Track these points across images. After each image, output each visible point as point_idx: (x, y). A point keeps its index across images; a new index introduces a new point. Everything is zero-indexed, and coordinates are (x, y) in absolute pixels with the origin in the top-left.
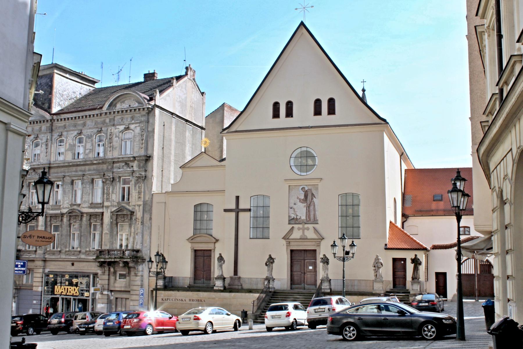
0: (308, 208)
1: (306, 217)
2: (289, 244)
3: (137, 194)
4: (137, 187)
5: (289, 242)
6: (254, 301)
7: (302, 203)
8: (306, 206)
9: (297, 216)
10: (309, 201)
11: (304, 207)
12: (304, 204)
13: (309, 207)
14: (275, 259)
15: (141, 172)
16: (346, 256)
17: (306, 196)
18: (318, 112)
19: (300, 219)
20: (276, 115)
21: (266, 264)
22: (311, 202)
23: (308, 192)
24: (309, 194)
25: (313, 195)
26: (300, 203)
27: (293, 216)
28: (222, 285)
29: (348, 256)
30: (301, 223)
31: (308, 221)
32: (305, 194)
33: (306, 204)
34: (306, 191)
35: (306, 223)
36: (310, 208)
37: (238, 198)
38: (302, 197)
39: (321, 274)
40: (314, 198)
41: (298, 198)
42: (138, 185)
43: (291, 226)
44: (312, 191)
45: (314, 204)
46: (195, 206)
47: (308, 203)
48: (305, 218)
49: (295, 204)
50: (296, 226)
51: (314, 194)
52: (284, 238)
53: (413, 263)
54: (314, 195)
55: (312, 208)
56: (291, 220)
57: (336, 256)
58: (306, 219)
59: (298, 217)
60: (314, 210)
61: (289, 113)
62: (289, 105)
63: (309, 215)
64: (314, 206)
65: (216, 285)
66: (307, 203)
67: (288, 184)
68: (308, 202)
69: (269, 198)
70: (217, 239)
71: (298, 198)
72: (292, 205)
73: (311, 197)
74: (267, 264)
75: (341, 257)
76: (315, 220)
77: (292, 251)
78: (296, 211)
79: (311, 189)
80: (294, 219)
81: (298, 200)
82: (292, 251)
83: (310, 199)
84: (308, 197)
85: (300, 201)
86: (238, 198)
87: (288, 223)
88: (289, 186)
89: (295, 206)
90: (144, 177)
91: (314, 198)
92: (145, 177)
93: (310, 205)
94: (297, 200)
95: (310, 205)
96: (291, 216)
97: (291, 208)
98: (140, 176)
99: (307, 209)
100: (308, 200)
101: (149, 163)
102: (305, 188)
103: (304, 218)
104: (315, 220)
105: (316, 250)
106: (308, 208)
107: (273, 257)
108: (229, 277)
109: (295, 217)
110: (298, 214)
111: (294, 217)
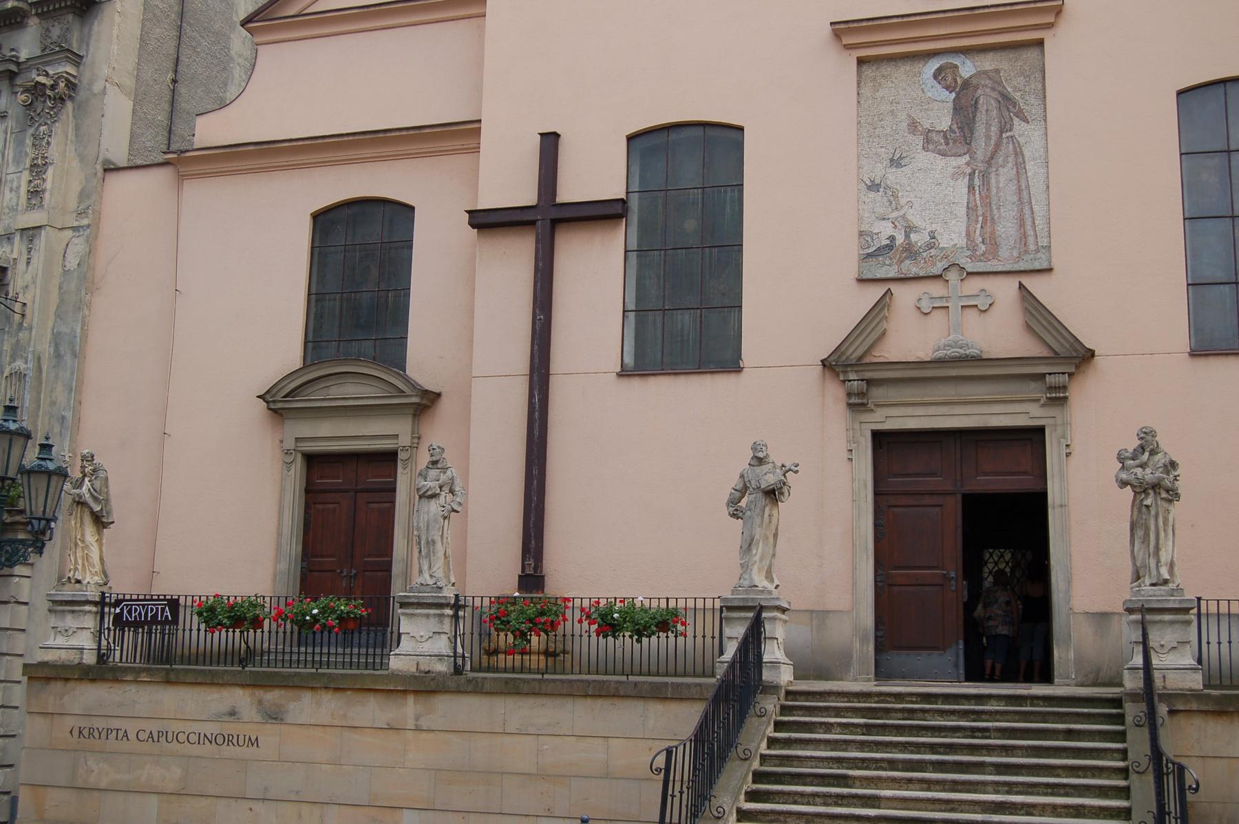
0: (977, 182)
1: (968, 235)
2: (858, 404)
3: (26, 176)
4: (29, 141)
5: (869, 382)
6: (669, 752)
7: (944, 155)
8: (968, 170)
9: (909, 229)
10: (988, 137)
11: (955, 176)
13: (985, 176)
15: (48, 63)
17: (965, 111)
19: (930, 246)
21: (733, 502)
22: (998, 145)
23: (976, 88)
25: (1006, 100)
26: (931, 155)
27: (885, 230)
30: (937, 270)
31: (984, 257)
33: (967, 157)
34: (966, 84)
36: (993, 176)
37: (550, 142)
38: (944, 121)
40: (1016, 121)
41: (913, 126)
42: (31, 131)
43: (876, 292)
44: (1000, 83)
45: (1018, 153)
46: (316, 217)
47: (980, 154)
48: (962, 242)
49: (896, 162)
50: (905, 296)
51: (1017, 96)
52: (833, 366)
54: (1015, 104)
55: (1003, 177)
56: (869, 255)
58: (971, 246)
59: (918, 239)
63: (989, 220)
64: (1020, 167)
67: (848, 47)
68: (981, 148)
69: (740, 146)
71: (913, 126)
72: (878, 171)
73: (995, 113)
74: (743, 503)
76: (1026, 252)
77: (881, 439)
78: (903, 201)
79: (997, 71)
80: (890, 247)
81: (919, 141)
82: (881, 439)
83: (994, 129)
84: (981, 117)
85: (928, 141)
86: (550, 142)
87: (854, 274)
88: (861, 62)
89: (894, 177)
90: (62, 85)
91: (1016, 121)
92: (71, 86)
93: (989, 161)
94: (910, 137)
95: (989, 161)
96: (871, 234)
97: (874, 187)
98: (42, 79)
99: (971, 188)
100: (980, 130)
101: (96, 23)
102: (956, 67)
103: (953, 236)
104: (1026, 252)
105: (1041, 430)
106: (977, 182)
109: (900, 239)
110: (916, 220)
111: (892, 238)
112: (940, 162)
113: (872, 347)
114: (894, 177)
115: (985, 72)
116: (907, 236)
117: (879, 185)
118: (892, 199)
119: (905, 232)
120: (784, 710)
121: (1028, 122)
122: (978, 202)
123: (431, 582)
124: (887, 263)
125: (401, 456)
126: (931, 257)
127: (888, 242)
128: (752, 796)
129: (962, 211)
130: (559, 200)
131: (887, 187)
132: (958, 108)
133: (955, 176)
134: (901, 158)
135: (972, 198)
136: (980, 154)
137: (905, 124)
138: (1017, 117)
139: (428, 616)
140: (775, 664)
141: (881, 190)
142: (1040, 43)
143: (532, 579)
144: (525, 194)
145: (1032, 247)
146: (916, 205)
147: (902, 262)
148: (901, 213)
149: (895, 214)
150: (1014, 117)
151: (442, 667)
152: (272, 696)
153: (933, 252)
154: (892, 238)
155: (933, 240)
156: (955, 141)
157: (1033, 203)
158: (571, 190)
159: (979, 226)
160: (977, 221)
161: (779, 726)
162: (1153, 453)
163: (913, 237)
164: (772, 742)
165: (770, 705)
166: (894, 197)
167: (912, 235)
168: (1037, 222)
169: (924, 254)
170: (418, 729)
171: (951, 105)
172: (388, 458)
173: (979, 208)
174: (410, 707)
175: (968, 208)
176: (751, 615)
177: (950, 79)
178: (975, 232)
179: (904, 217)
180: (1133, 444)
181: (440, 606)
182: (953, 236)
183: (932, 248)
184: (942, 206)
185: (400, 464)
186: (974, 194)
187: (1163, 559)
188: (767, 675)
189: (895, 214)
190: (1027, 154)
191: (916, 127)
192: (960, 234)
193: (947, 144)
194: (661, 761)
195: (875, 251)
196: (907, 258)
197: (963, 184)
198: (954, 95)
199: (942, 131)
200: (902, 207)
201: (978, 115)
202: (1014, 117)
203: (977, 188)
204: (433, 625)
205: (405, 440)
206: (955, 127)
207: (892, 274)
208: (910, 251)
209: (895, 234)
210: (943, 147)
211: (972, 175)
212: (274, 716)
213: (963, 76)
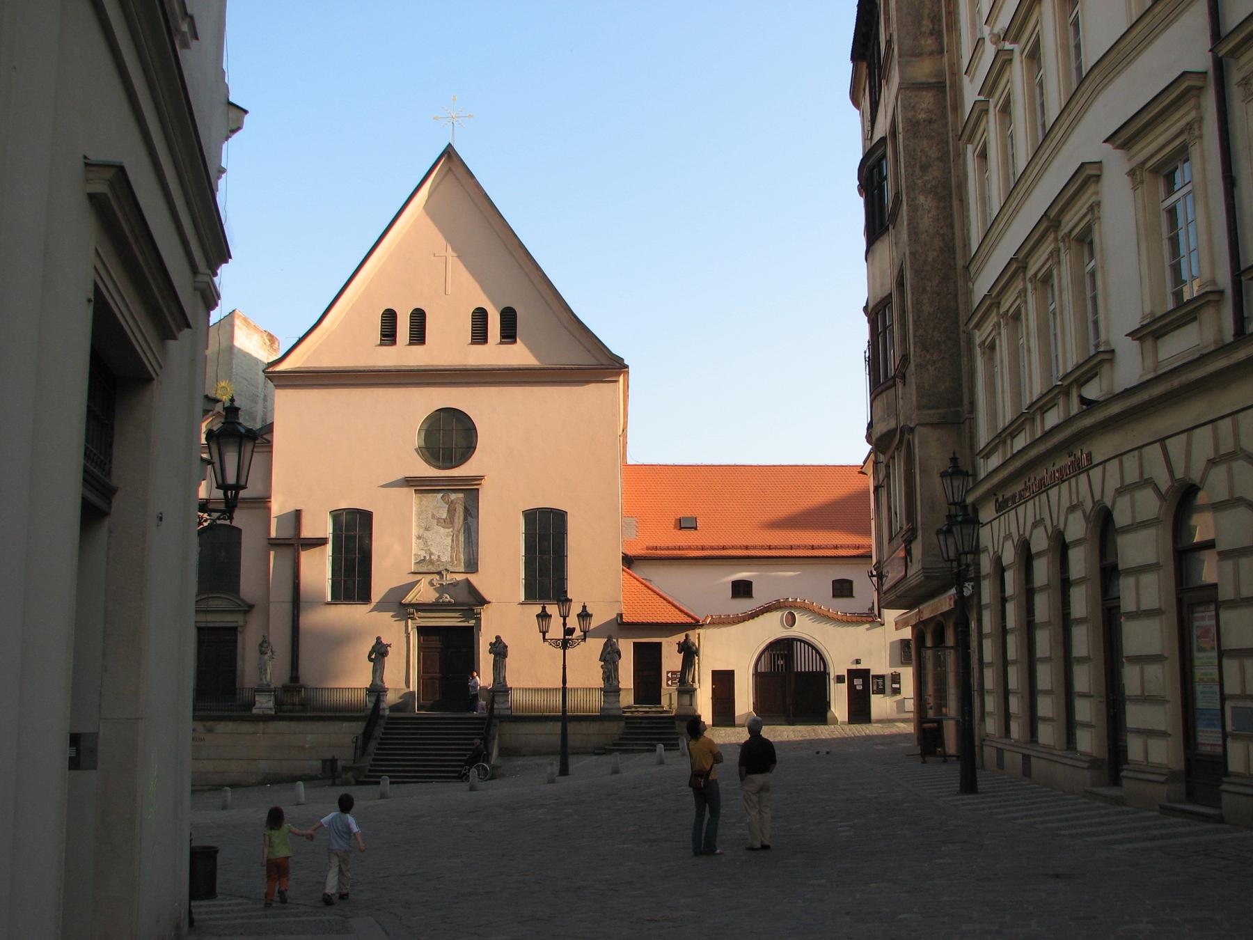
0: (455, 538)
6: (357, 737)
9: (431, 554)
12: (447, 530)
14: (389, 646)
16: (567, 637)
18: (480, 334)
19: (438, 560)
20: (389, 334)
21: (369, 657)
28: (271, 704)
29: (570, 637)
31: (456, 566)
33: (451, 529)
34: (452, 502)
35: (451, 569)
38: (445, 515)
39: (484, 678)
49: (427, 529)
51: (470, 508)
53: (681, 653)
57: (546, 638)
60: (469, 542)
61: (418, 334)
62: (419, 318)
65: (258, 705)
66: (453, 527)
70: (250, 601)
71: (433, 516)
74: (373, 657)
75: (559, 640)
76: (470, 564)
78: (429, 543)
80: (424, 560)
81: (436, 521)
84: (457, 514)
85: (438, 522)
88: (415, 490)
94: (432, 520)
99: (453, 540)
100: (456, 520)
103: (445, 558)
106: (455, 538)
107: (385, 641)
108: (281, 686)
109: (428, 558)
110: (434, 551)
111: (425, 557)
114: (427, 534)
116: (430, 557)
120: (387, 723)
123: (265, 683)
125: (239, 629)
127: (423, 558)
128: (378, 749)
129: (449, 549)
130: (302, 536)
133: (447, 536)
136: (456, 529)
137: (430, 515)
139: (265, 695)
140: (384, 709)
142: (478, 489)
143: (295, 677)
144: (288, 533)
145: (472, 563)
151: (273, 712)
152: (209, 724)
153: (439, 563)
154: (425, 557)
158: (307, 533)
161: (385, 728)
162: (500, 643)
163: (432, 557)
164: (383, 734)
165: (382, 722)
166: (426, 543)
170: (264, 733)
172: (233, 631)
174: (261, 726)
176: (376, 694)
179: (429, 549)
180: (494, 640)
181: (270, 691)
182: (445, 558)
185: (239, 633)
187: (501, 676)
188: (381, 713)
194: (355, 740)
204: (267, 698)
205: (241, 623)
207: (425, 570)
208: (431, 562)
211: (453, 536)
212: (210, 730)
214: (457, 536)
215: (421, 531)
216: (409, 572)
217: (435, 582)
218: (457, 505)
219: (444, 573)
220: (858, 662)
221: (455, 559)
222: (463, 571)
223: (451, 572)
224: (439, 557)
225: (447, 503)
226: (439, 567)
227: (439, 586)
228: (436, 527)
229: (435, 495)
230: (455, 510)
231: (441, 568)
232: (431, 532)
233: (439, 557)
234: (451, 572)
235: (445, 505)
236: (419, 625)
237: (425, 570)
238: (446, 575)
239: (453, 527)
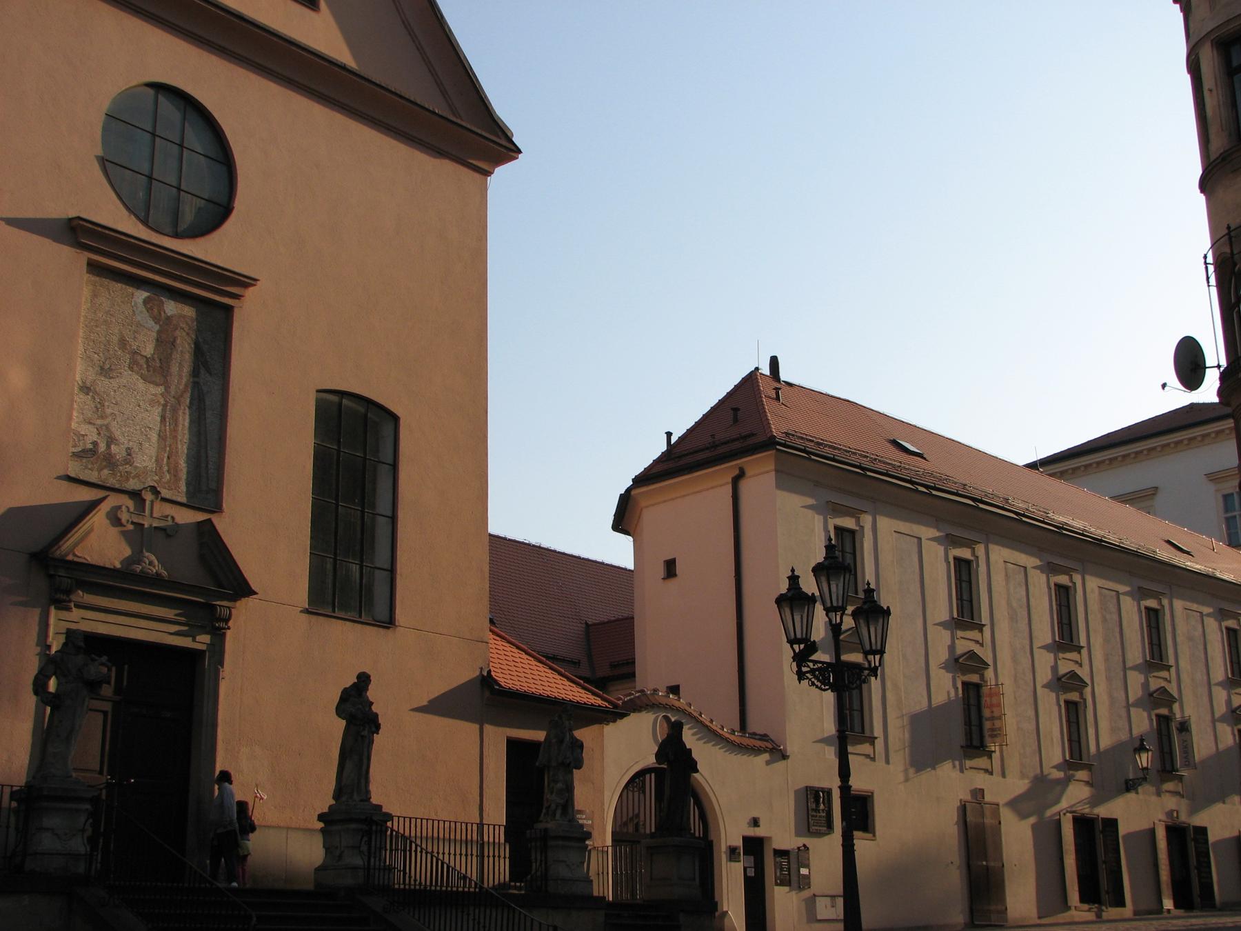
0: (168, 414)
9: (111, 440)
24: (178, 341)
32: (159, 332)
33: (161, 389)
34: (168, 318)
38: (149, 350)
40: (202, 371)
41: (123, 343)
49: (105, 371)
66: (167, 388)
71: (123, 343)
78: (109, 411)
84: (176, 356)
89: (103, 384)
91: (202, 371)
97: (85, 389)
99: (163, 418)
100: (175, 369)
106: (168, 414)
109: (102, 447)
110: (117, 434)
111: (95, 444)
112: (141, 385)
113: (76, 545)
114: (103, 384)
115: (184, 317)
116: (108, 446)
117: (89, 389)
118: (99, 406)
119: (107, 442)
121: (210, 374)
122: (168, 433)
124: (90, 467)
126: (127, 472)
127: (91, 446)
131: (96, 393)
132: (159, 341)
133: (152, 403)
134: (110, 369)
135: (163, 428)
138: (204, 366)
141: (91, 394)
146: (119, 419)
147: (102, 469)
148: (106, 422)
149: (99, 422)
150: (201, 366)
153: (128, 468)
154: (95, 444)
155: (129, 457)
156: (154, 371)
157: (209, 448)
159: (166, 455)
160: (165, 450)
167: (112, 446)
168: (209, 466)
169: (121, 468)
171: (155, 334)
173: (168, 439)
175: (159, 435)
177: (156, 310)
178: (163, 460)
179: (107, 427)
183: (127, 464)
184: (138, 428)
186: (165, 426)
189: (99, 422)
190: (207, 403)
191: (126, 344)
192: (151, 457)
193: (148, 371)
195: (80, 451)
196: (105, 467)
197: (157, 411)
198: (157, 327)
199: (146, 357)
200: (107, 417)
201: (175, 353)
202: (201, 366)
203: (167, 420)
206: (156, 356)
207: (93, 479)
208: (109, 461)
209: (99, 441)
210: (144, 372)
211: (165, 406)
213: (167, 312)
214: (175, 411)
215: (91, 375)
216: (62, 473)
217: (124, 517)
218: (178, 333)
219: (148, 497)
220: (755, 822)
221: (166, 468)
222: (184, 500)
223: (165, 500)
224: (129, 452)
225: (156, 319)
226: (128, 479)
227: (131, 527)
228: (127, 373)
229: (130, 290)
230: (173, 343)
231: (133, 485)
232: (114, 383)
233: (129, 452)
234: (165, 500)
235: (151, 323)
236: (73, 626)
237: (93, 477)
238: (152, 502)
239: (167, 388)
